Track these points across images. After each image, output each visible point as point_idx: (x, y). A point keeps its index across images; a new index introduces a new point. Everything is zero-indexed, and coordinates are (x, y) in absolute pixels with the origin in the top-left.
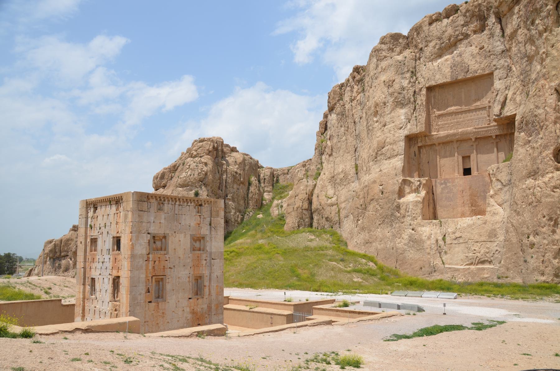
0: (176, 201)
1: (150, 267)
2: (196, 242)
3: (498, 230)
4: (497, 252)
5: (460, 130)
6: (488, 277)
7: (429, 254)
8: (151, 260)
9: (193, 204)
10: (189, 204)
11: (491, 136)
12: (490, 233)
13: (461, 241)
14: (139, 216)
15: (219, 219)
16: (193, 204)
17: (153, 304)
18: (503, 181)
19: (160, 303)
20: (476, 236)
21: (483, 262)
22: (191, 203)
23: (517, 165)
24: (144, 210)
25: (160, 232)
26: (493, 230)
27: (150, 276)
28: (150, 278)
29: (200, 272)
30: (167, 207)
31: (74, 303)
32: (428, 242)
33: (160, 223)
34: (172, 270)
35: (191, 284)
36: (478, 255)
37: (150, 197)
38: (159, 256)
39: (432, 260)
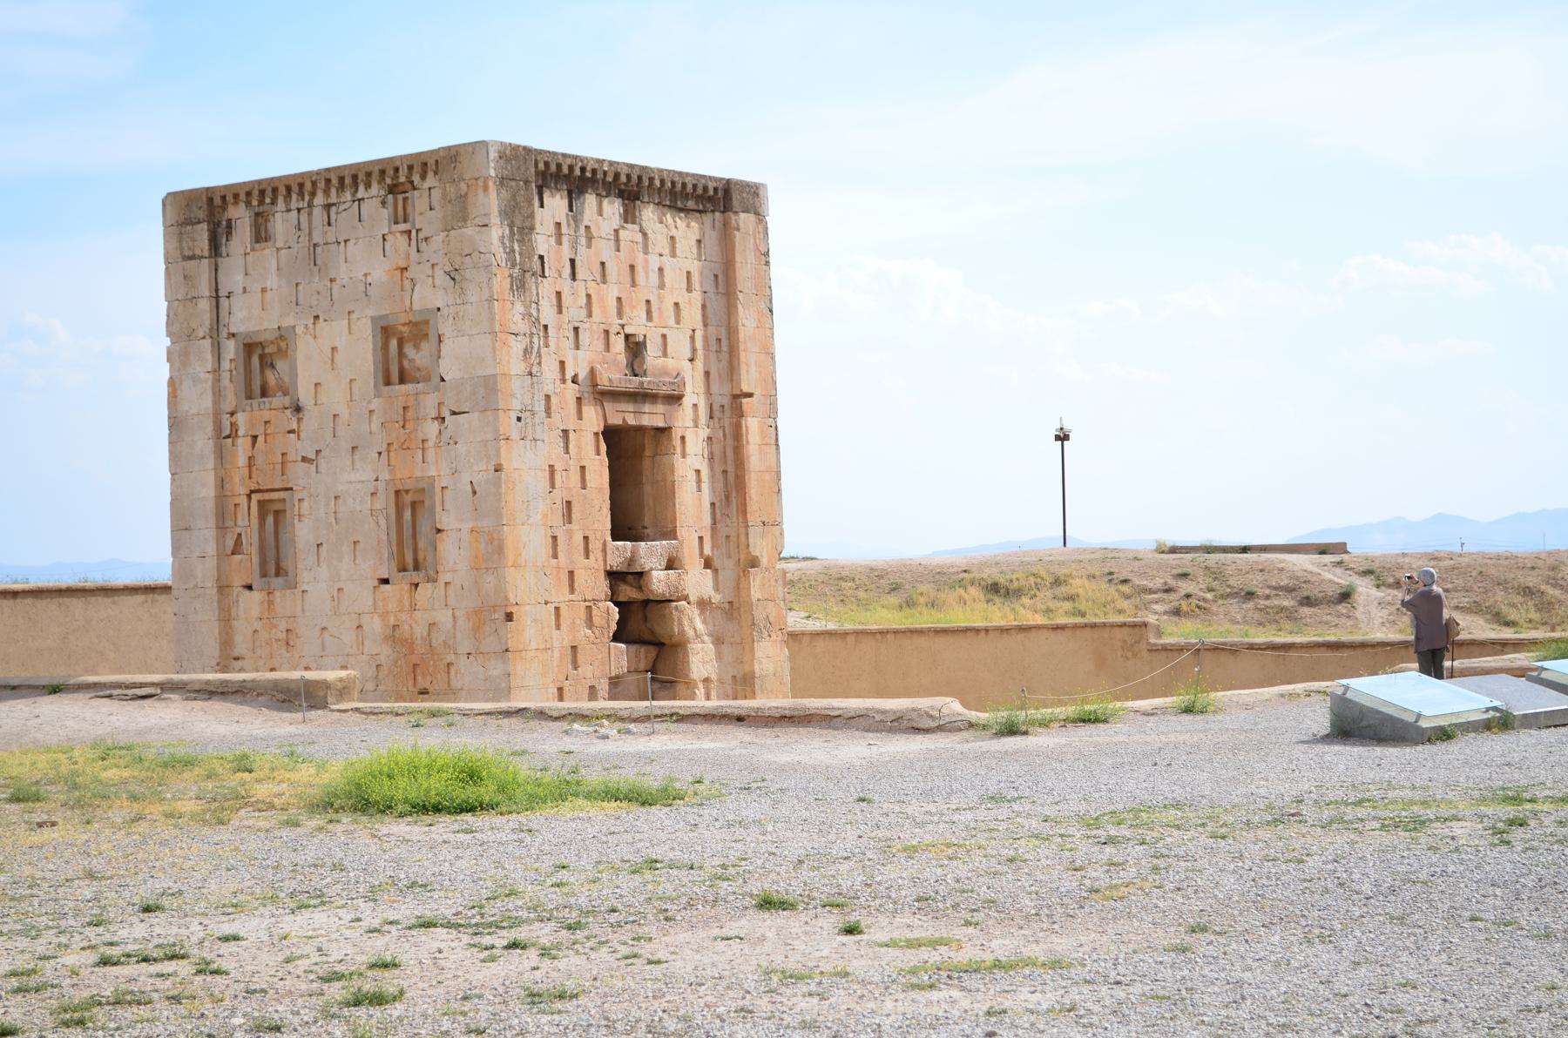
0: (313, 194)
1: (242, 461)
2: (417, 347)
8: (240, 433)
9: (375, 189)
10: (361, 193)
14: (185, 277)
15: (469, 231)
16: (375, 187)
17: (256, 596)
19: (277, 594)
22: (368, 186)
24: (198, 253)
25: (266, 325)
27: (243, 491)
28: (243, 500)
29: (419, 474)
30: (281, 223)
31: (170, 583)
33: (264, 290)
34: (313, 468)
35: (383, 522)
37: (218, 201)
38: (267, 415)
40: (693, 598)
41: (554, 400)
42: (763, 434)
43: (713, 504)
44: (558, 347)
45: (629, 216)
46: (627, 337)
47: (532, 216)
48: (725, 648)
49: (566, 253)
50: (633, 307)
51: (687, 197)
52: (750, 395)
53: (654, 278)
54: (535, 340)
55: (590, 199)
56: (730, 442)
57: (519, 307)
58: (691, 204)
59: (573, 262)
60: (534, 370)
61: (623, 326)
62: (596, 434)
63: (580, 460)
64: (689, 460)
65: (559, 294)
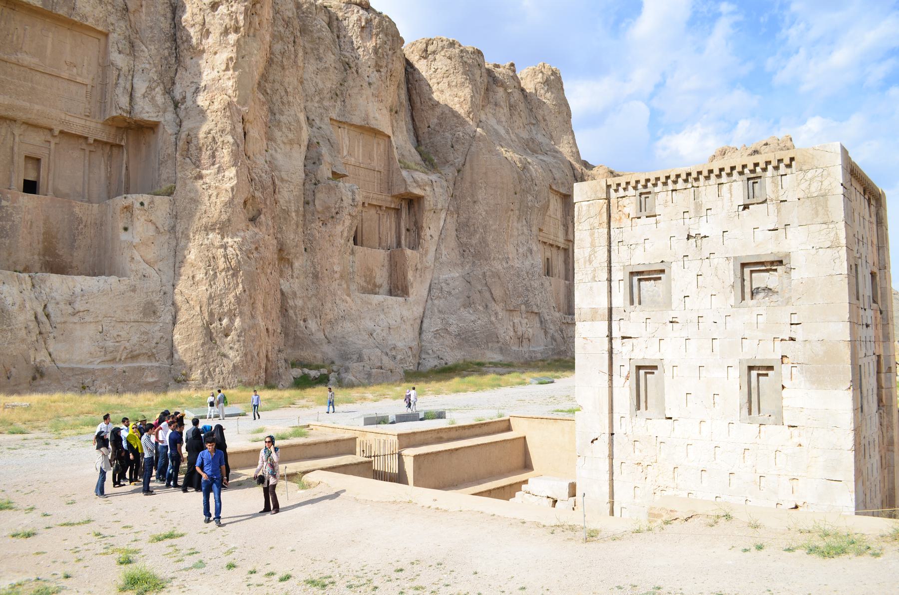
3: (156, 304)
4: (163, 341)
5: (37, 107)
6: (156, 382)
7: (23, 341)
11: (86, 138)
12: (145, 309)
13: (88, 319)
18: (160, 226)
20: (119, 312)
21: (134, 357)
23: (188, 206)
26: (148, 303)
32: (21, 318)
36: (127, 345)
39: (32, 353)
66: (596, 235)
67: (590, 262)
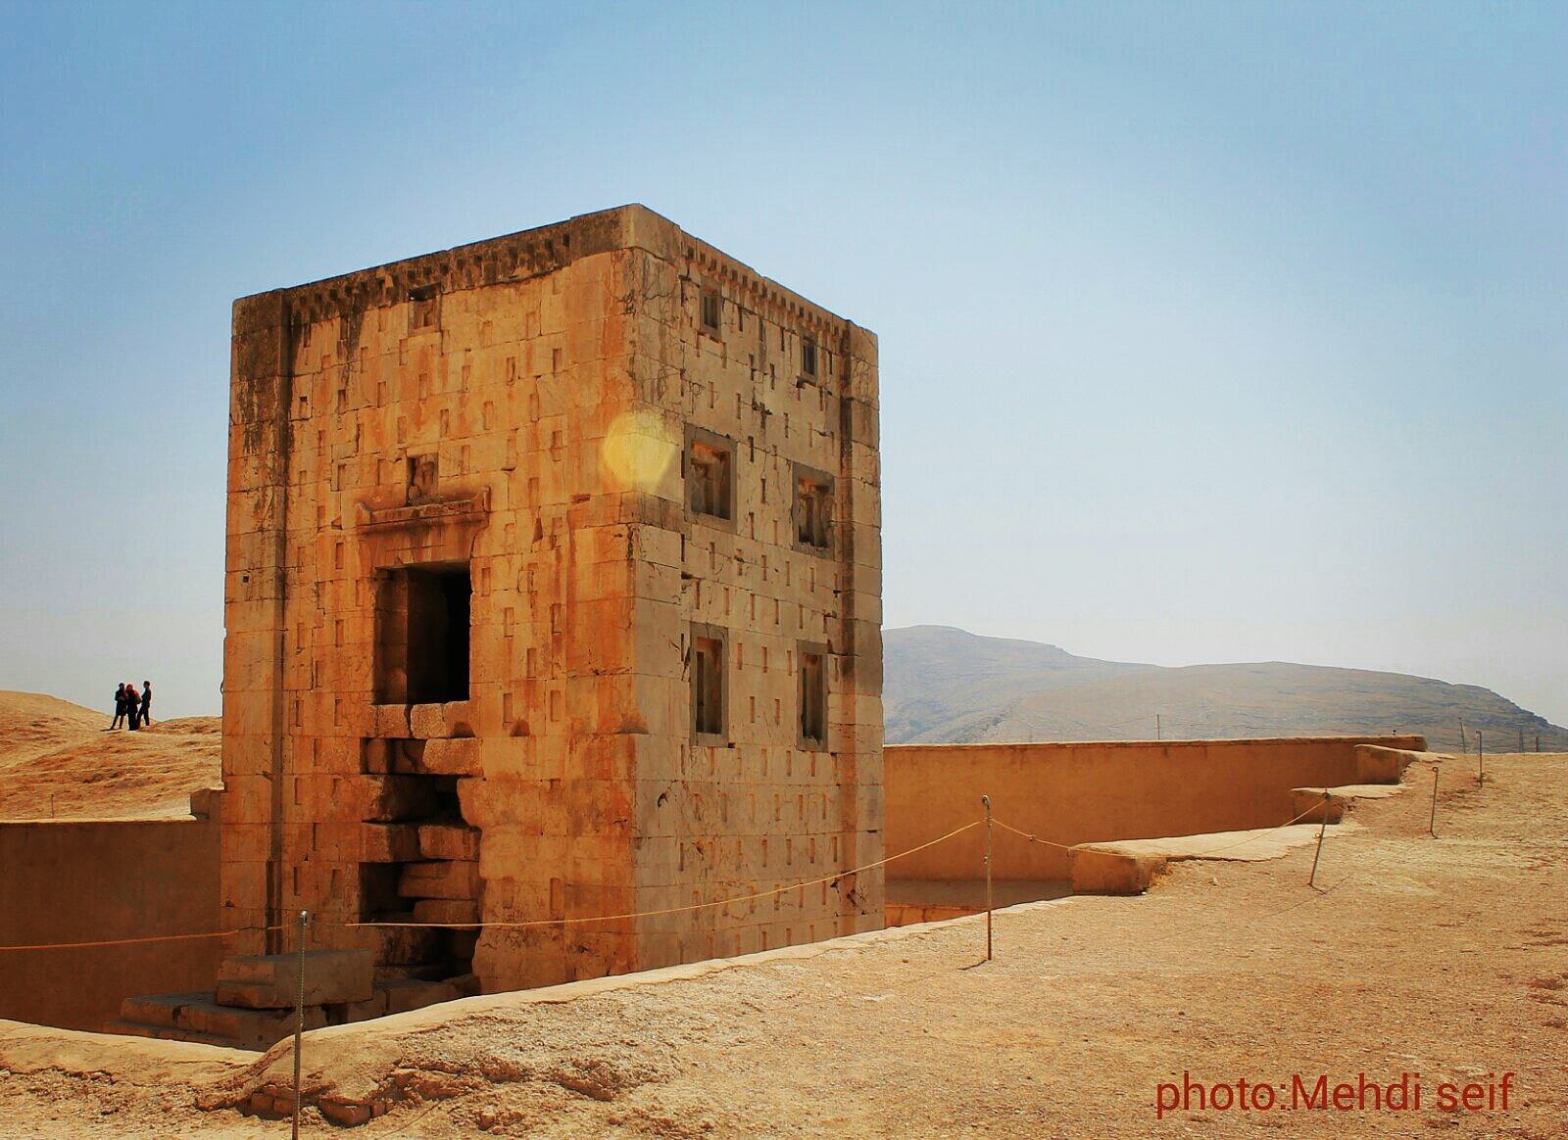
40: (486, 774)
41: (309, 551)
42: (602, 547)
43: (530, 652)
44: (317, 489)
45: (427, 317)
46: (413, 463)
47: (275, 361)
48: (544, 843)
49: (335, 384)
50: (419, 424)
51: (514, 268)
52: (586, 498)
53: (454, 382)
54: (269, 492)
55: (371, 316)
56: (565, 563)
57: (254, 462)
58: (521, 272)
59: (342, 393)
60: (265, 525)
61: (404, 450)
62: (362, 579)
63: (337, 612)
64: (492, 599)
65: (321, 435)
66: (668, 336)
67: (660, 397)
